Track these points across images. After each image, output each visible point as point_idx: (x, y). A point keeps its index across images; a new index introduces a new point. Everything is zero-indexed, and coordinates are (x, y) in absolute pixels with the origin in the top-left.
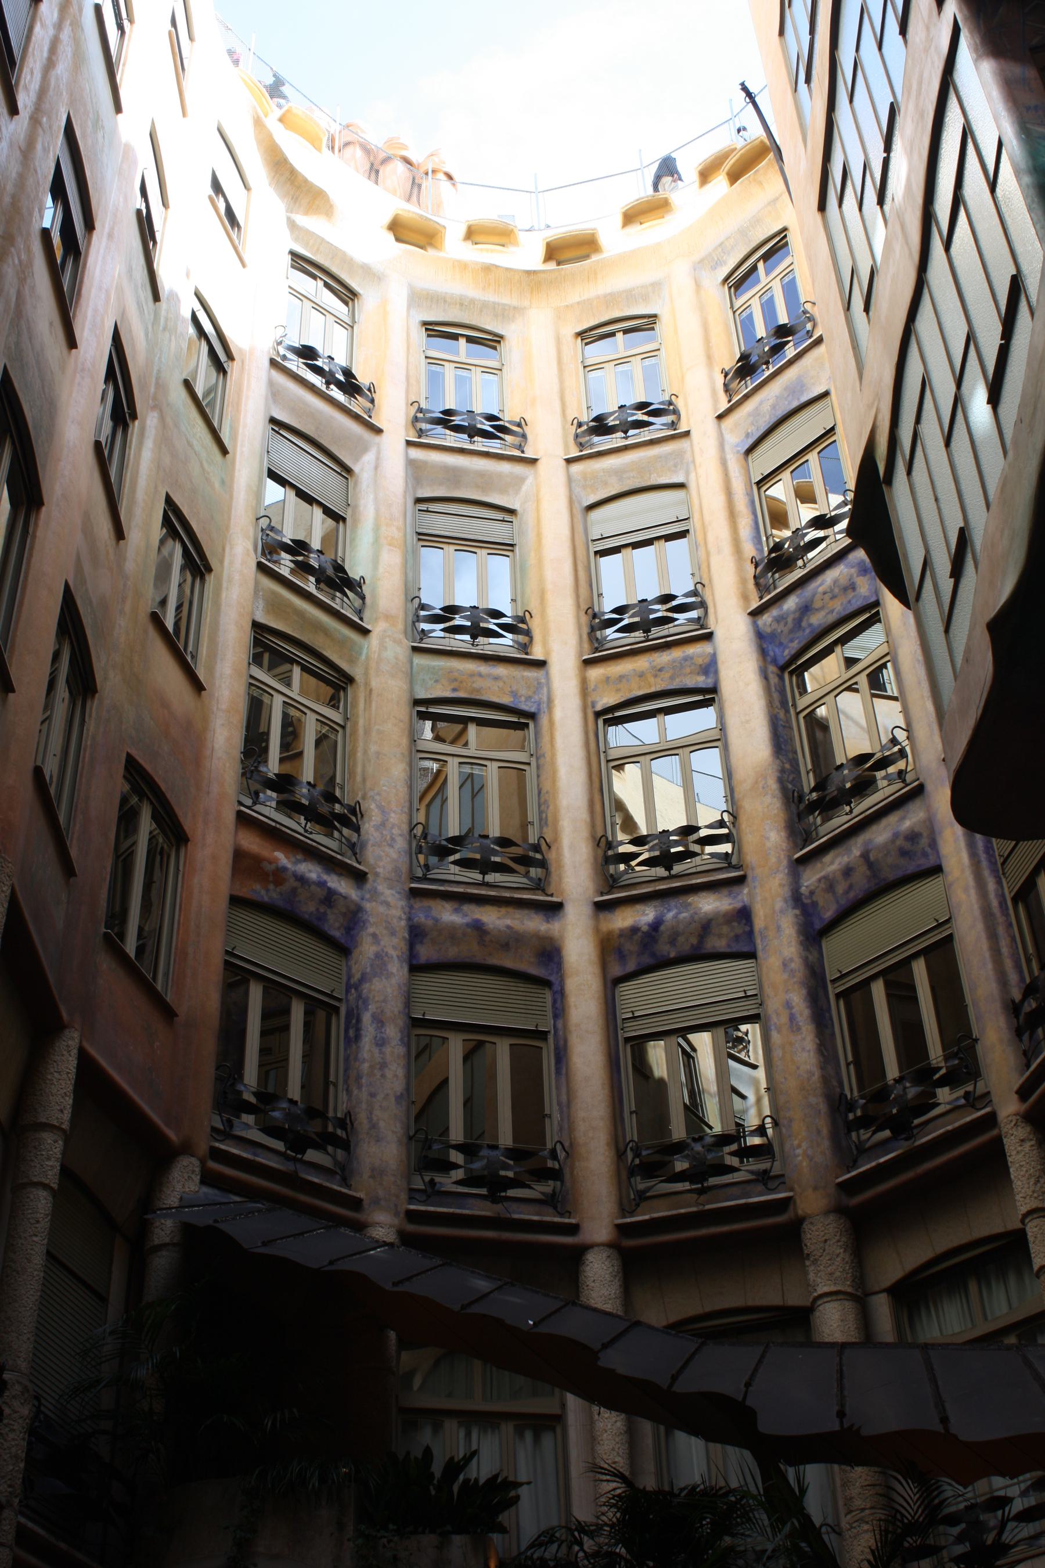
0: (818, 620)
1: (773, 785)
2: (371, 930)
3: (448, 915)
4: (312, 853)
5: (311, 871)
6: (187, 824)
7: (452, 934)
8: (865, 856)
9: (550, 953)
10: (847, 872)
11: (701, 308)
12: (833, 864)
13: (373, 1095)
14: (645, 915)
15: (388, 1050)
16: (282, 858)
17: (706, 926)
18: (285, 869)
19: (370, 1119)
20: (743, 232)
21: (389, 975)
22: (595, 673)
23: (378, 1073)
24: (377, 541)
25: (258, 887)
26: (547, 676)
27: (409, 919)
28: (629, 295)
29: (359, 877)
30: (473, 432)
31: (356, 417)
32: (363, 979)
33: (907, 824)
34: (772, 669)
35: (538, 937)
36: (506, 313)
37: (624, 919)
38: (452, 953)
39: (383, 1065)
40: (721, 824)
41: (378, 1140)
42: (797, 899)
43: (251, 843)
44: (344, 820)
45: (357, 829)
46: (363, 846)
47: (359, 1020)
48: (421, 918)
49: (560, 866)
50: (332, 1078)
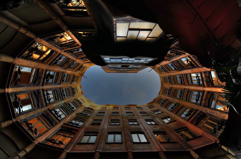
0: (179, 66)
1: (192, 69)
2: (202, 110)
3: (203, 102)
4: (193, 114)
5: (195, 115)
6: (185, 126)
7: (205, 102)
8: (196, 61)
9: (209, 92)
10: (198, 62)
11: (163, 74)
12: (198, 64)
13: (219, 116)
14: (205, 82)
15: (215, 112)
16: (193, 118)
17: (206, 76)
18: (194, 118)
19: (222, 117)
20: (158, 71)
21: (207, 110)
22: (186, 84)
23: (217, 114)
24: (174, 101)
25: (195, 121)
26: (186, 88)
27: (203, 106)
28: (163, 79)
29: (198, 110)
30: (169, 92)
31: (167, 101)
32: (207, 113)
33: (192, 57)
34: (184, 69)
35: (206, 93)
36: (164, 87)
37: (205, 84)
38: (207, 102)
39: (216, 113)
40: (196, 74)
41: (225, 117)
42: (202, 67)
43: (190, 120)
44: (193, 110)
45: (193, 109)
46: (195, 109)
47: (211, 115)
48: (203, 105)
49: (200, 90)
50: (218, 119)
